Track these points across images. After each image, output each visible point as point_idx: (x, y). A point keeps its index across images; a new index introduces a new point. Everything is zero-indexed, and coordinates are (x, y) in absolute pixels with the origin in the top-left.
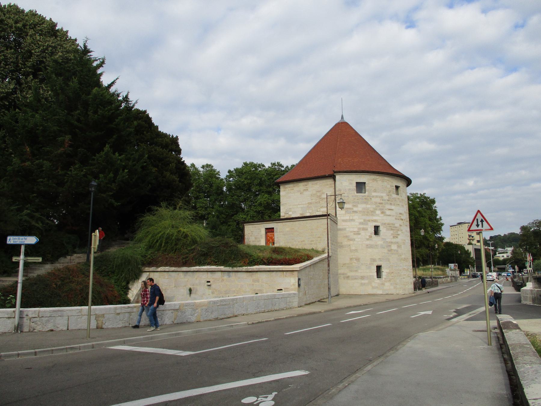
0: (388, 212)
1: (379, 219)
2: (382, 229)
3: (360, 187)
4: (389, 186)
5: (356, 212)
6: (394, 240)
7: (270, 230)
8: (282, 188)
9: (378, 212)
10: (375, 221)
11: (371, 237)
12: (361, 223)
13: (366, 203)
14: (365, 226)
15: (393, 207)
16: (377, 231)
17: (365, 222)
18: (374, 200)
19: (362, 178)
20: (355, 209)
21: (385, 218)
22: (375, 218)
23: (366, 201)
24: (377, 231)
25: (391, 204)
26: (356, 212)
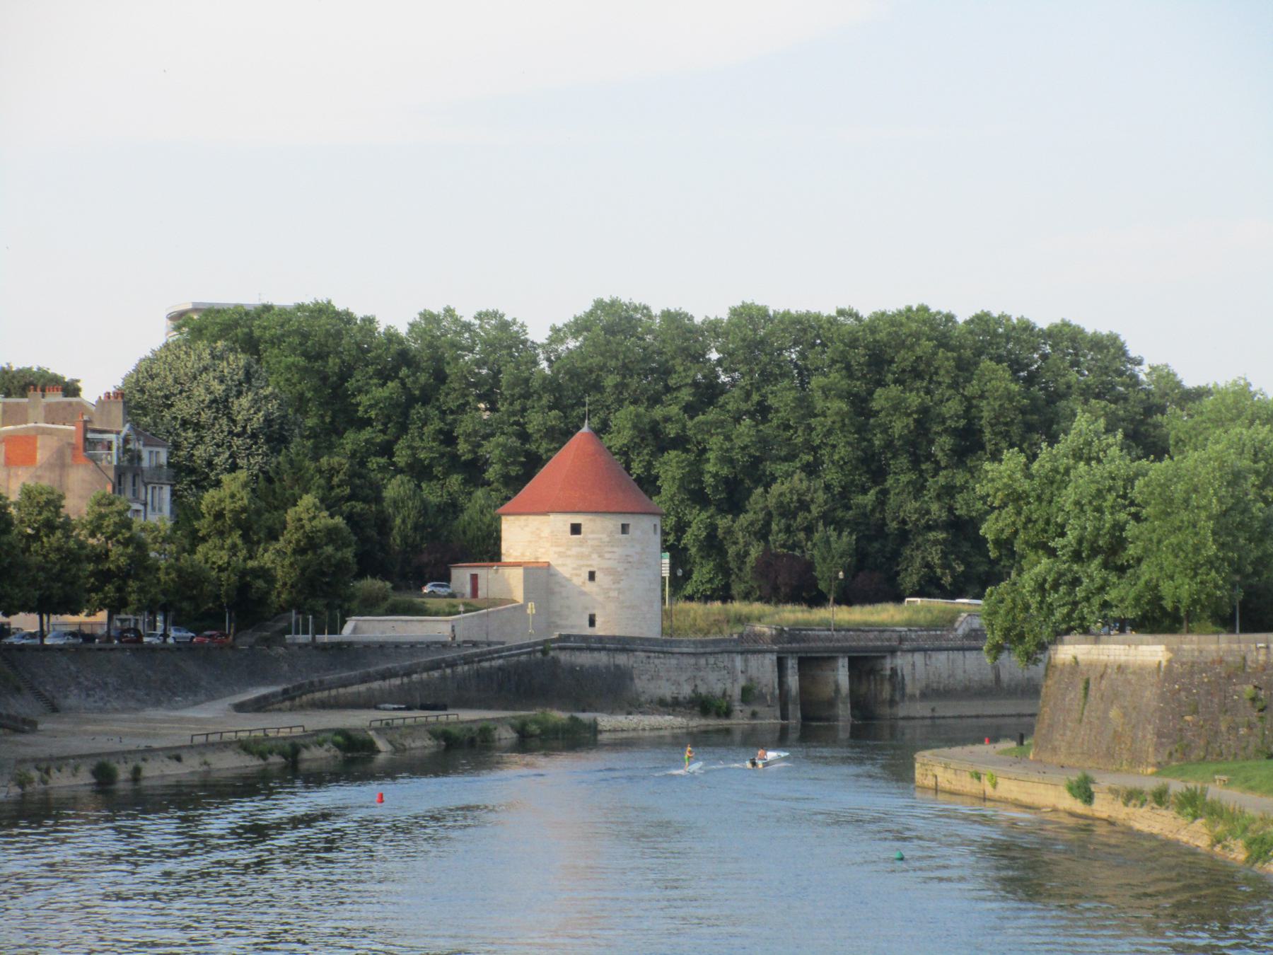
0: (607, 556)
1: (595, 563)
2: (597, 575)
3: (576, 529)
5: (569, 556)
7: (474, 578)
8: (503, 518)
9: (595, 556)
10: (591, 566)
11: (584, 583)
12: (574, 569)
13: (581, 546)
14: (578, 572)
16: (592, 576)
17: (579, 567)
18: (590, 542)
19: (577, 519)
20: (569, 553)
22: (589, 563)
23: (581, 544)
24: (592, 576)
25: (612, 546)
26: (569, 556)
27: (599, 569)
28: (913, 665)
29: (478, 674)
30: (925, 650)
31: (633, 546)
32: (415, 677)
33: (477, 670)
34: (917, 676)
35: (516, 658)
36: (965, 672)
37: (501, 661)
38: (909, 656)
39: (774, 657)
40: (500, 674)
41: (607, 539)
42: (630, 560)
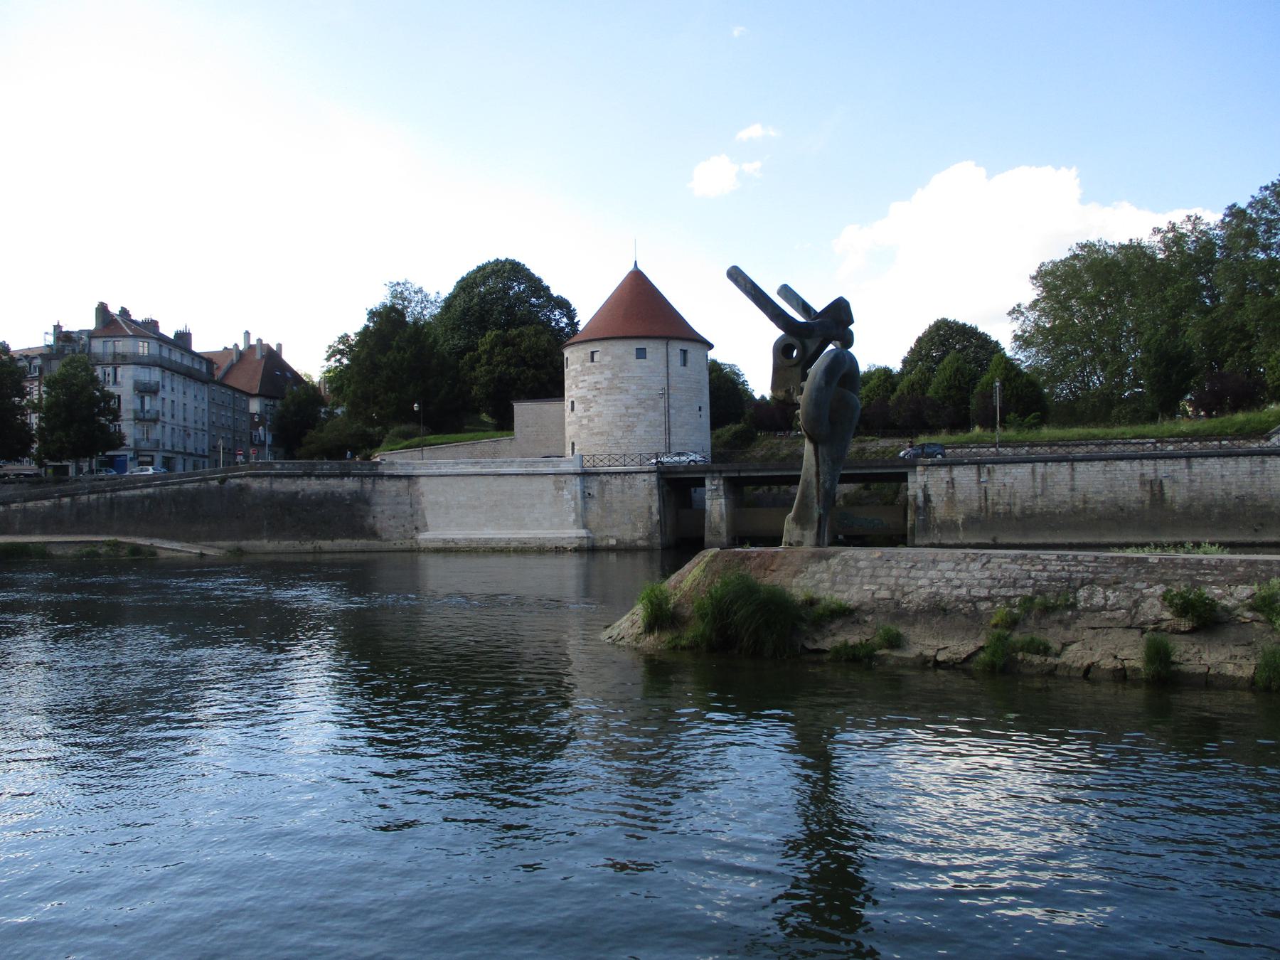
0: (581, 385)
4: (583, 355)
6: (585, 414)
15: (586, 378)
21: (581, 391)
25: (584, 375)
27: (577, 398)
28: (951, 483)
29: (112, 503)
30: (979, 464)
31: (602, 373)
32: (14, 506)
33: (111, 498)
34: (960, 496)
35: (177, 487)
36: (1073, 489)
37: (150, 490)
38: (943, 473)
39: (654, 478)
40: (147, 503)
41: (580, 369)
42: (598, 386)
